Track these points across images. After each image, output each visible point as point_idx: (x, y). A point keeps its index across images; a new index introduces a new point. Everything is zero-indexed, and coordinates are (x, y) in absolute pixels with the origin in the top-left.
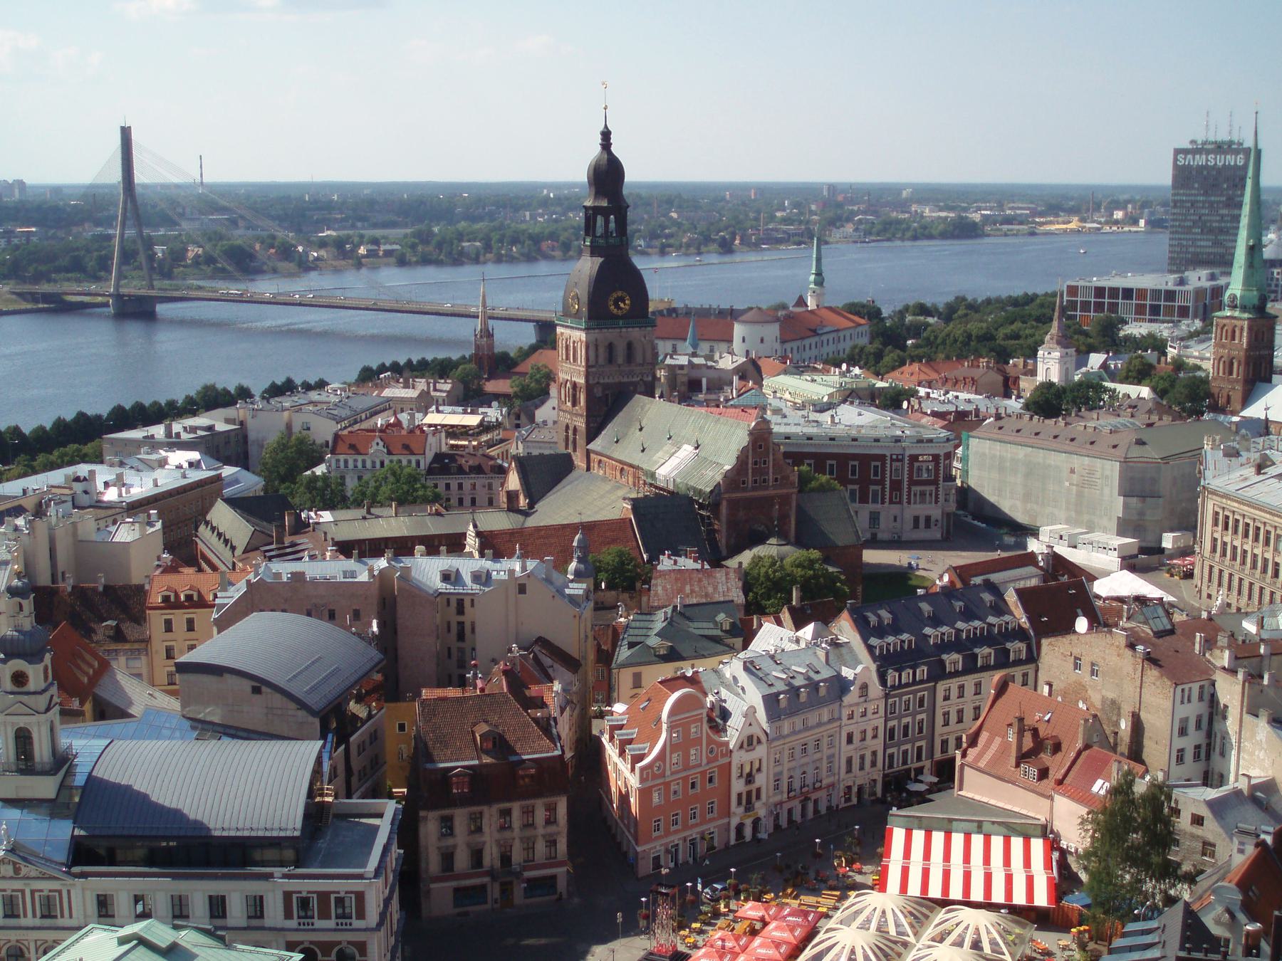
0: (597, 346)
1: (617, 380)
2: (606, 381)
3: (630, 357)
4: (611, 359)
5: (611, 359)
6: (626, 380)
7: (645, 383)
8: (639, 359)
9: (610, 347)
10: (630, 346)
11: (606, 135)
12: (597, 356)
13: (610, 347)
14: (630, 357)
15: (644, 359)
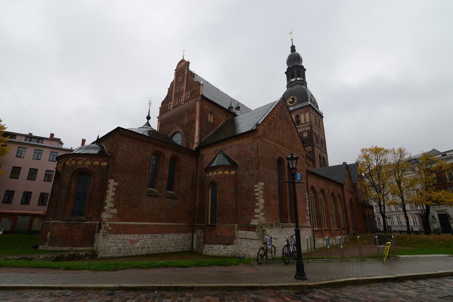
8: (302, 121)
11: (293, 48)
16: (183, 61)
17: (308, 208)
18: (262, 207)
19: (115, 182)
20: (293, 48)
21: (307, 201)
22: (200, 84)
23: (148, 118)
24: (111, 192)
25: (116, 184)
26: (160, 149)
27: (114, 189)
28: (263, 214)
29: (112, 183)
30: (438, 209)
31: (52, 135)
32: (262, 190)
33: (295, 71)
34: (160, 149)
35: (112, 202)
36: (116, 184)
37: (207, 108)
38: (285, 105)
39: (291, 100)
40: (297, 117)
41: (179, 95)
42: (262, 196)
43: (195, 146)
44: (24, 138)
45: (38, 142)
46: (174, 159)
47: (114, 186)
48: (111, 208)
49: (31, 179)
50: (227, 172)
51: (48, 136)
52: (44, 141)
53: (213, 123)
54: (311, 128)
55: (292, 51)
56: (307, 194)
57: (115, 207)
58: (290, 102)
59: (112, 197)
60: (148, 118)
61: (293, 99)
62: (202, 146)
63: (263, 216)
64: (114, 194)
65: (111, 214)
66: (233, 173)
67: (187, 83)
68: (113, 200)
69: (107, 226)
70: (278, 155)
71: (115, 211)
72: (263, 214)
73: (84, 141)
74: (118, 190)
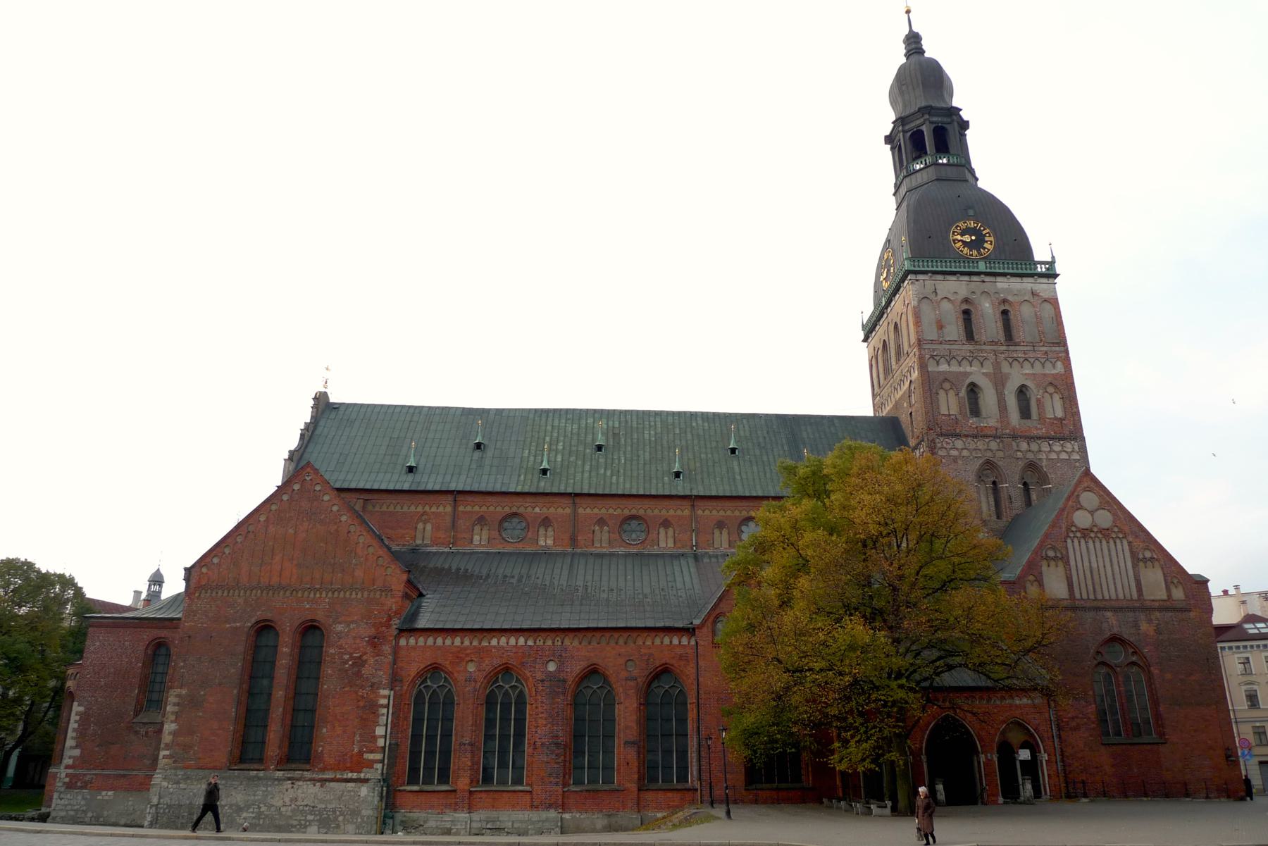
8: (906, 347)
11: (913, 43)
20: (913, 43)
24: (73, 725)
25: (81, 709)
28: (167, 753)
32: (175, 705)
36: (81, 709)
42: (173, 718)
48: (71, 748)
55: (908, 55)
56: (385, 692)
57: (76, 747)
59: (74, 730)
64: (76, 726)
68: (74, 734)
69: (63, 775)
70: (258, 615)
71: (77, 752)
72: (167, 753)
74: (84, 719)
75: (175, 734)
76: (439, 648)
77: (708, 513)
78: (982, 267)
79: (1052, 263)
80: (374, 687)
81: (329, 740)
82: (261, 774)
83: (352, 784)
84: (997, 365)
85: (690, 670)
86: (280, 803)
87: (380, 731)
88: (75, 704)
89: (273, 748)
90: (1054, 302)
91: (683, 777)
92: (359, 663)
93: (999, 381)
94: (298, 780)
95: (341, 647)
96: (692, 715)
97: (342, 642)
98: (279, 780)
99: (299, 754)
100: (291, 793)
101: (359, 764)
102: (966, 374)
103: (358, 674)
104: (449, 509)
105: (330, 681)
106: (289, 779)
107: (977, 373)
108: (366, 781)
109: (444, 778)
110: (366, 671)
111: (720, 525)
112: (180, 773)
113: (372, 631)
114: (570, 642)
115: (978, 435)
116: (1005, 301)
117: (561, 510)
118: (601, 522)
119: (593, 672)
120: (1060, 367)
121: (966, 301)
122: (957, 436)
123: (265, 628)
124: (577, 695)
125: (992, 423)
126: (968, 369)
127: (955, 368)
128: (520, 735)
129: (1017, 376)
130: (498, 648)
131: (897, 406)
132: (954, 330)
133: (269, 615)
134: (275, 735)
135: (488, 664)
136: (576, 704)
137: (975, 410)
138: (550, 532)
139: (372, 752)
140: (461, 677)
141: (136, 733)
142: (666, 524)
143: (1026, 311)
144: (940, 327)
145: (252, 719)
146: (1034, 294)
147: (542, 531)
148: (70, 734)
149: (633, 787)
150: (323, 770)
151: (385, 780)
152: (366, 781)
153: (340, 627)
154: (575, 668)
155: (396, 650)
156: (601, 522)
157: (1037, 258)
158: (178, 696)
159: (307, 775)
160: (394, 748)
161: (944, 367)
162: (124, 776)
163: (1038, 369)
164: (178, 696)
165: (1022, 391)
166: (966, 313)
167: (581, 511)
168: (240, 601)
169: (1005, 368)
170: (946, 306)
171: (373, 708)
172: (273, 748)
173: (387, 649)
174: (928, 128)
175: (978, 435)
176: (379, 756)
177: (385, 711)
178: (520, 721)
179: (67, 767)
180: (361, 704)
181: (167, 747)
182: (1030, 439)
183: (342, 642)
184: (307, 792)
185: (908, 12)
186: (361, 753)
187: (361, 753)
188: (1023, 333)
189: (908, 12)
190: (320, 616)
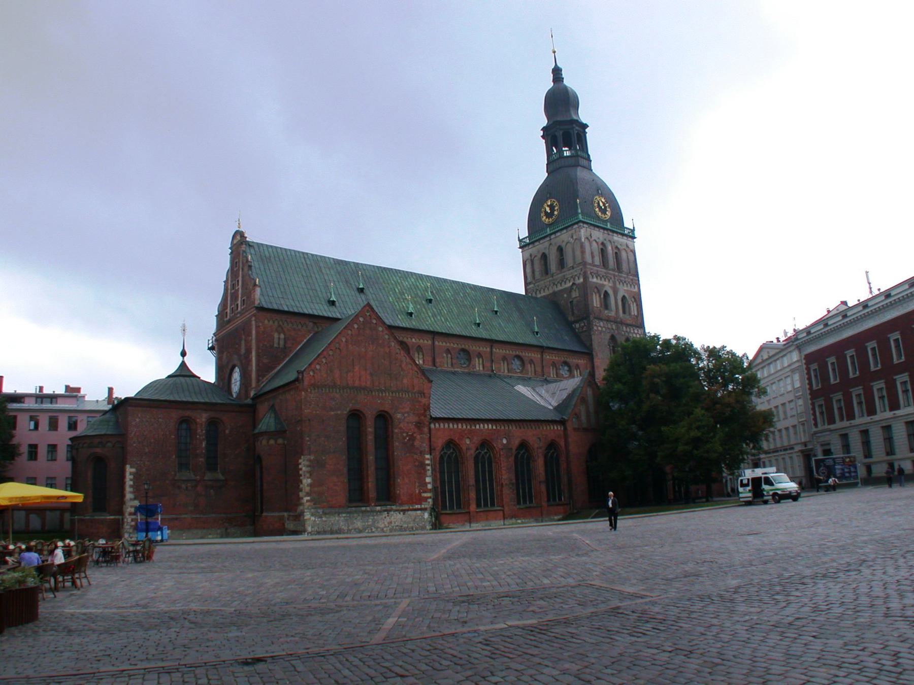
0: (532, 261)
1: (551, 291)
2: (543, 294)
3: (561, 263)
4: (546, 271)
5: (546, 271)
6: (560, 288)
7: (578, 285)
8: (569, 262)
9: (544, 257)
10: (560, 250)
11: (557, 73)
12: (533, 272)
13: (544, 257)
14: (561, 263)
15: (574, 262)
16: (237, 233)
17: (428, 480)
18: (308, 489)
19: (131, 467)
21: (429, 468)
22: (255, 285)
23: (183, 354)
25: (133, 470)
26: (188, 413)
27: (132, 477)
28: (309, 498)
29: (129, 470)
30: (822, 439)
31: (67, 387)
32: (308, 466)
33: (559, 134)
34: (188, 413)
35: (131, 492)
36: (133, 470)
37: (271, 322)
38: (373, 316)
39: (548, 210)
40: (560, 250)
41: (234, 297)
42: (308, 475)
43: (252, 394)
44: (34, 399)
45: (51, 403)
46: (213, 423)
47: (131, 474)
48: (131, 499)
49: (52, 460)
50: (272, 442)
51: (62, 391)
52: (59, 400)
53: (285, 347)
54: (585, 278)
55: (554, 81)
56: (428, 456)
57: (135, 499)
58: (548, 215)
59: (131, 486)
60: (183, 354)
61: (552, 207)
62: (257, 397)
63: (307, 501)
64: (132, 483)
65: (131, 507)
66: (280, 441)
67: (243, 277)
68: (132, 489)
69: (129, 520)
70: (350, 406)
72: (309, 498)
73: (111, 390)
74: (137, 477)
75: (311, 485)
76: (451, 430)
77: (498, 351)
78: (609, 226)
79: (633, 231)
80: (422, 453)
81: (403, 486)
82: (368, 509)
83: (419, 512)
84: (614, 283)
85: (562, 443)
86: (383, 526)
87: (428, 480)
88: (128, 467)
89: (372, 494)
90: (634, 252)
91: (560, 499)
92: (412, 438)
93: (616, 292)
94: (408, 510)
95: (401, 428)
96: (563, 466)
97: (402, 425)
98: (380, 511)
99: (387, 496)
100: (388, 519)
101: (421, 500)
102: (603, 286)
103: (413, 445)
104: (488, 349)
105: (398, 449)
106: (385, 511)
107: (607, 285)
108: (425, 509)
109: (459, 507)
110: (417, 443)
111: (504, 358)
112: (320, 511)
113: (416, 419)
114: (513, 428)
115: (608, 320)
116: (617, 247)
117: (426, 342)
118: (448, 351)
119: (523, 445)
120: (636, 290)
121: (603, 244)
122: (600, 319)
123: (356, 416)
124: (516, 456)
125: (613, 314)
126: (606, 283)
127: (599, 281)
128: (491, 480)
129: (623, 290)
130: (480, 430)
131: (554, 293)
132: (597, 260)
133: (358, 407)
134: (371, 484)
135: (477, 440)
136: (516, 463)
137: (606, 306)
138: (421, 356)
139: (425, 492)
140: (464, 448)
141: (179, 487)
142: (480, 355)
143: (624, 254)
144: (593, 257)
145: (356, 474)
146: (627, 246)
147: (416, 355)
148: (128, 489)
149: (544, 504)
150: (401, 504)
151: (433, 509)
152: (425, 509)
153: (399, 416)
154: (516, 442)
155: (430, 429)
156: (448, 351)
157: (625, 225)
158: (310, 460)
159: (394, 507)
160: (435, 489)
161: (595, 280)
162: (176, 519)
163: (629, 288)
164: (310, 460)
165: (624, 298)
166: (602, 249)
167: (436, 343)
168: (338, 396)
169: (618, 286)
170: (594, 244)
171: (423, 465)
172: (372, 494)
173: (426, 430)
174: (564, 129)
175: (608, 320)
176: (429, 495)
177: (429, 468)
178: (490, 472)
179: (130, 514)
180: (417, 463)
181: (308, 494)
182: (627, 325)
183: (402, 425)
184: (397, 518)
185: (554, 52)
186: (420, 493)
187: (420, 493)
188: (625, 267)
189: (554, 52)
190: (387, 408)
